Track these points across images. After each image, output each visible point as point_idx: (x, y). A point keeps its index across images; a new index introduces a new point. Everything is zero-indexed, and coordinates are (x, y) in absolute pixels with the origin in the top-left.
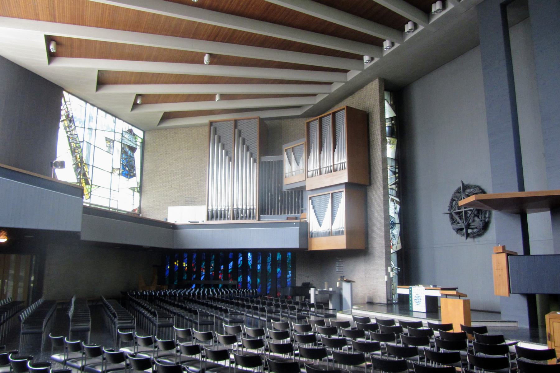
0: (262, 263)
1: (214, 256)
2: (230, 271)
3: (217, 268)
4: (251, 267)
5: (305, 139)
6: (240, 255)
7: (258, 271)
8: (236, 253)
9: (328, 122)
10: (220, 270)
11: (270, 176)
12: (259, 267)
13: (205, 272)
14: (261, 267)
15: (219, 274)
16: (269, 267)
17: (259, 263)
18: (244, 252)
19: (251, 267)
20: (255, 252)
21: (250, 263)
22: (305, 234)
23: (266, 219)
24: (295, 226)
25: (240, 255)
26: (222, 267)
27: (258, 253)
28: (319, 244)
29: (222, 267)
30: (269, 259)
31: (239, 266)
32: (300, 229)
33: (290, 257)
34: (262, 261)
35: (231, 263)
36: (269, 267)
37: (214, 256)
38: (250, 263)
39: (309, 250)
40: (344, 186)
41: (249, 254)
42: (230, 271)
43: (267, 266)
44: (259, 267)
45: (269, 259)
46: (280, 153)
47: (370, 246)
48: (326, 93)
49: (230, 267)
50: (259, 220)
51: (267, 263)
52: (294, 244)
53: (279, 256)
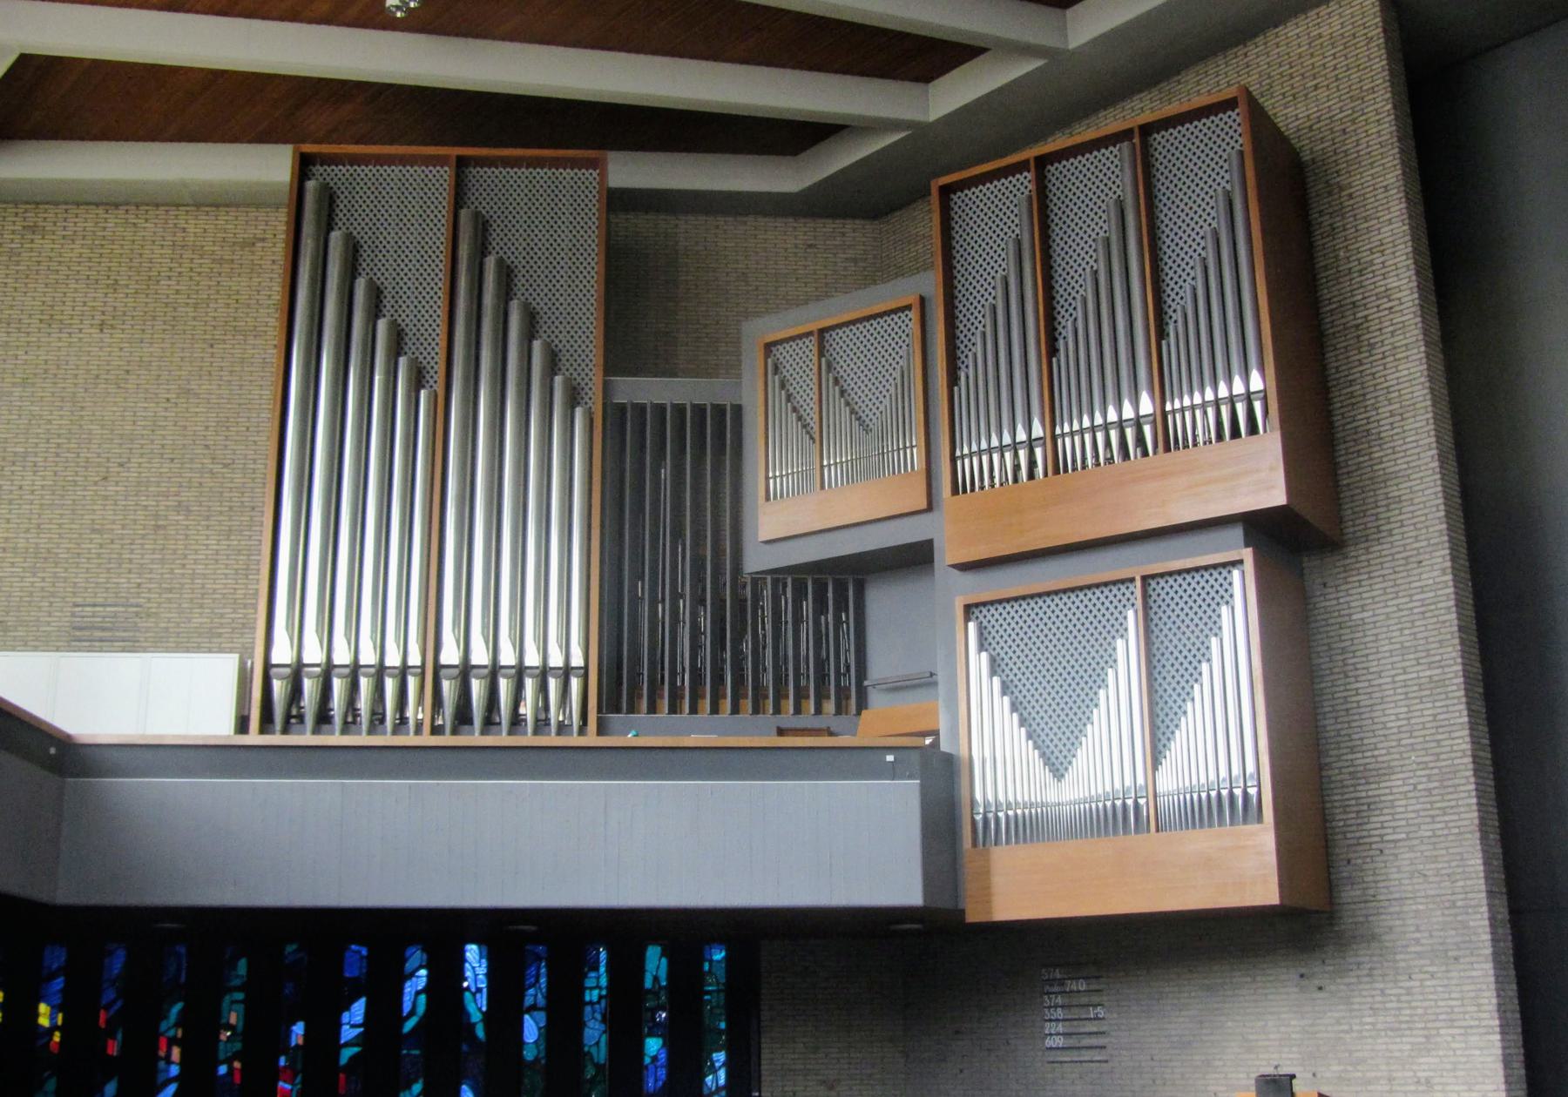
0: (550, 1009)
1: (242, 967)
2: (346, 1054)
3: (262, 1037)
4: (480, 1032)
5: (930, 283)
6: (416, 956)
7: (529, 1054)
8: (394, 933)
9: (1094, 190)
10: (285, 1048)
11: (662, 484)
12: (531, 1029)
13: (183, 1063)
14: (549, 1033)
15: (276, 1074)
16: (595, 1034)
17: (533, 1008)
18: (441, 931)
19: (480, 1032)
20: (507, 931)
21: (476, 1006)
22: (948, 826)
23: (632, 732)
24: (893, 772)
25: (416, 956)
26: (299, 1029)
27: (518, 935)
28: (1017, 891)
29: (299, 1029)
30: (597, 984)
31: (409, 1025)
32: (922, 786)
33: (721, 973)
34: (549, 996)
35: (358, 1010)
36: (595, 1034)
37: (242, 967)
38: (476, 1006)
39: (971, 917)
40: (1237, 533)
41: (472, 951)
42: (346, 1054)
43: (580, 1026)
44: (531, 1029)
45: (597, 984)
46: (717, 356)
47: (1348, 894)
48: (1027, 50)
49: (348, 1033)
50: (602, 730)
51: (582, 1003)
52: (896, 883)
53: (656, 964)
